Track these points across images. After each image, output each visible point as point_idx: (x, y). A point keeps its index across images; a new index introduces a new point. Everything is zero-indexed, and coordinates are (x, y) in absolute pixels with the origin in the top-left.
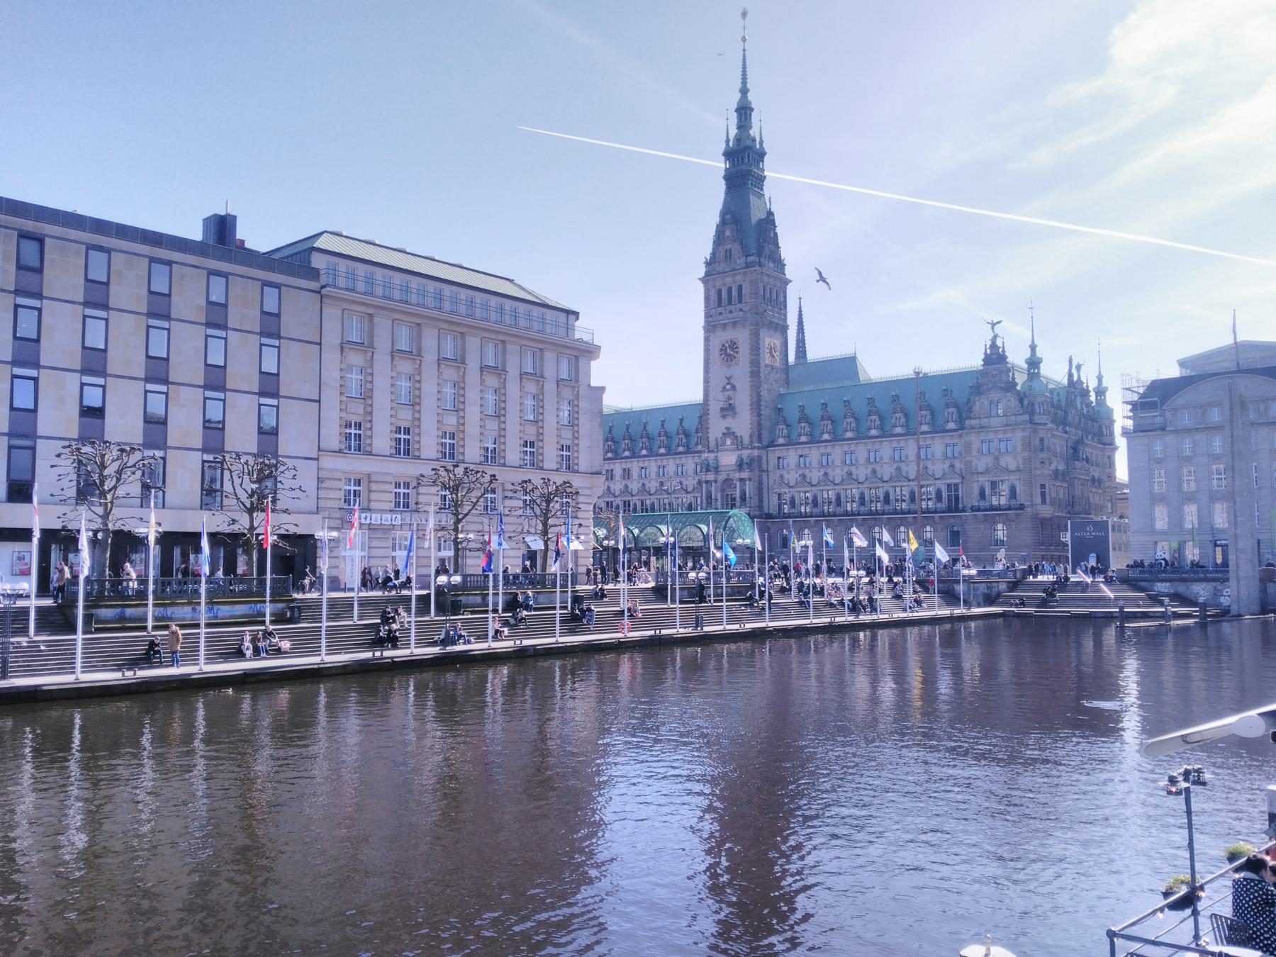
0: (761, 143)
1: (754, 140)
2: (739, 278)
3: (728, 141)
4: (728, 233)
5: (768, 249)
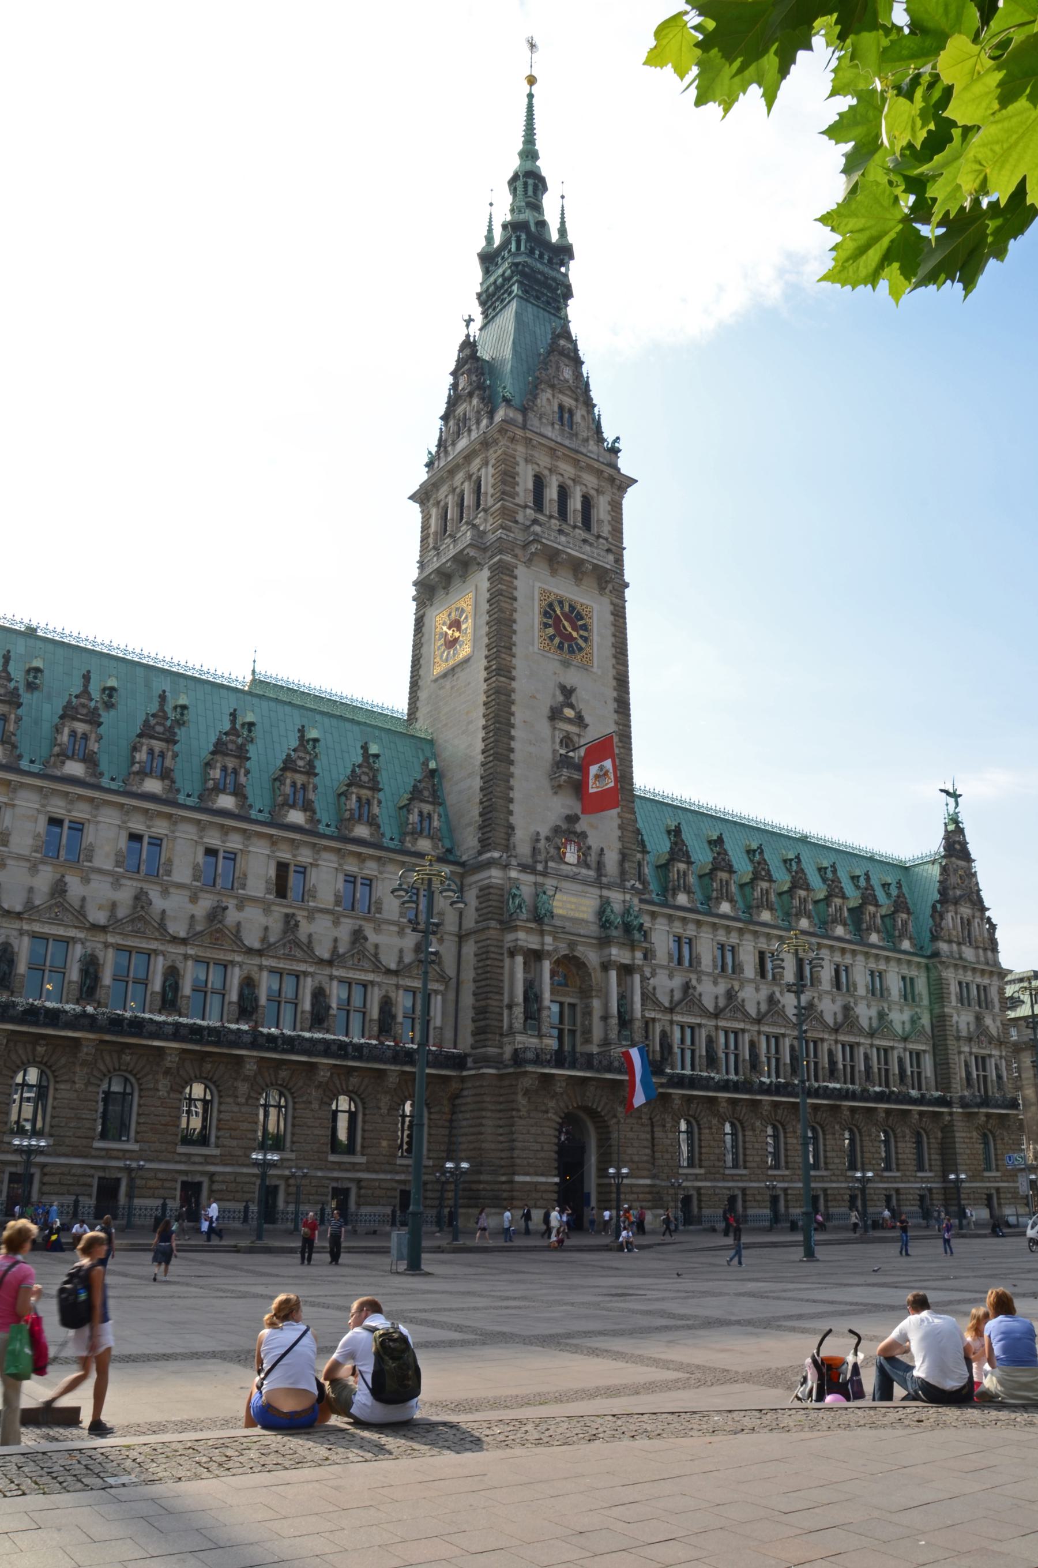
0: (563, 231)
1: (542, 224)
2: (477, 462)
3: (489, 239)
4: (463, 382)
5: (547, 401)
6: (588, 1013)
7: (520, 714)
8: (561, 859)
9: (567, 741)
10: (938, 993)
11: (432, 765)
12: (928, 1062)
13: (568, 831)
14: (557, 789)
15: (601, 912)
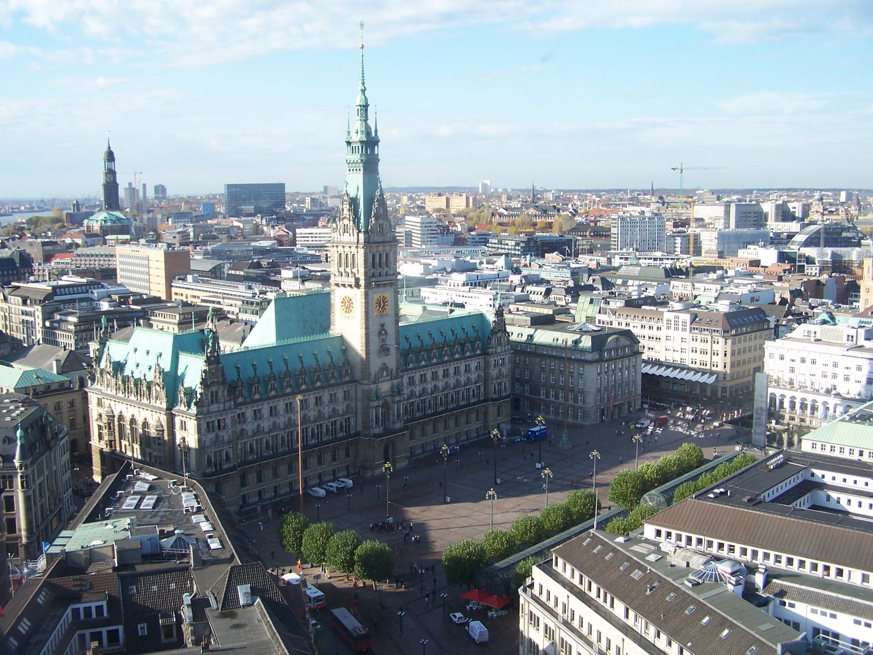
0: (376, 131)
6: (389, 414)
7: (371, 338)
8: (382, 374)
9: (383, 340)
10: (487, 366)
11: (344, 348)
12: (482, 388)
13: (384, 368)
14: (380, 357)
15: (392, 388)
